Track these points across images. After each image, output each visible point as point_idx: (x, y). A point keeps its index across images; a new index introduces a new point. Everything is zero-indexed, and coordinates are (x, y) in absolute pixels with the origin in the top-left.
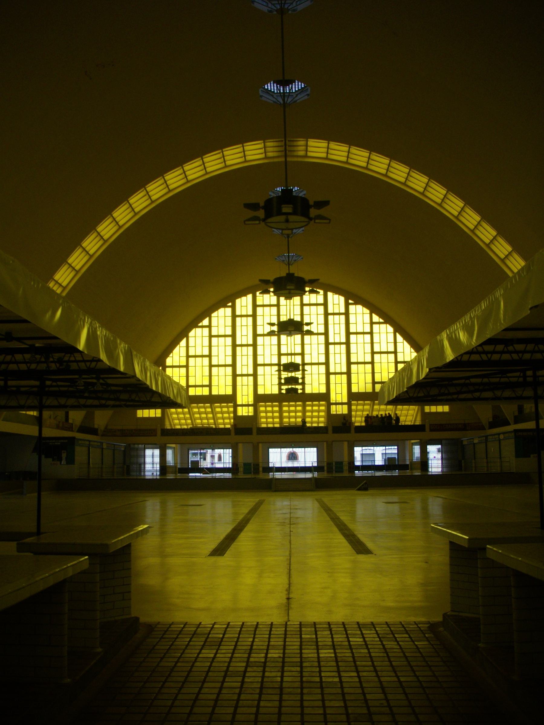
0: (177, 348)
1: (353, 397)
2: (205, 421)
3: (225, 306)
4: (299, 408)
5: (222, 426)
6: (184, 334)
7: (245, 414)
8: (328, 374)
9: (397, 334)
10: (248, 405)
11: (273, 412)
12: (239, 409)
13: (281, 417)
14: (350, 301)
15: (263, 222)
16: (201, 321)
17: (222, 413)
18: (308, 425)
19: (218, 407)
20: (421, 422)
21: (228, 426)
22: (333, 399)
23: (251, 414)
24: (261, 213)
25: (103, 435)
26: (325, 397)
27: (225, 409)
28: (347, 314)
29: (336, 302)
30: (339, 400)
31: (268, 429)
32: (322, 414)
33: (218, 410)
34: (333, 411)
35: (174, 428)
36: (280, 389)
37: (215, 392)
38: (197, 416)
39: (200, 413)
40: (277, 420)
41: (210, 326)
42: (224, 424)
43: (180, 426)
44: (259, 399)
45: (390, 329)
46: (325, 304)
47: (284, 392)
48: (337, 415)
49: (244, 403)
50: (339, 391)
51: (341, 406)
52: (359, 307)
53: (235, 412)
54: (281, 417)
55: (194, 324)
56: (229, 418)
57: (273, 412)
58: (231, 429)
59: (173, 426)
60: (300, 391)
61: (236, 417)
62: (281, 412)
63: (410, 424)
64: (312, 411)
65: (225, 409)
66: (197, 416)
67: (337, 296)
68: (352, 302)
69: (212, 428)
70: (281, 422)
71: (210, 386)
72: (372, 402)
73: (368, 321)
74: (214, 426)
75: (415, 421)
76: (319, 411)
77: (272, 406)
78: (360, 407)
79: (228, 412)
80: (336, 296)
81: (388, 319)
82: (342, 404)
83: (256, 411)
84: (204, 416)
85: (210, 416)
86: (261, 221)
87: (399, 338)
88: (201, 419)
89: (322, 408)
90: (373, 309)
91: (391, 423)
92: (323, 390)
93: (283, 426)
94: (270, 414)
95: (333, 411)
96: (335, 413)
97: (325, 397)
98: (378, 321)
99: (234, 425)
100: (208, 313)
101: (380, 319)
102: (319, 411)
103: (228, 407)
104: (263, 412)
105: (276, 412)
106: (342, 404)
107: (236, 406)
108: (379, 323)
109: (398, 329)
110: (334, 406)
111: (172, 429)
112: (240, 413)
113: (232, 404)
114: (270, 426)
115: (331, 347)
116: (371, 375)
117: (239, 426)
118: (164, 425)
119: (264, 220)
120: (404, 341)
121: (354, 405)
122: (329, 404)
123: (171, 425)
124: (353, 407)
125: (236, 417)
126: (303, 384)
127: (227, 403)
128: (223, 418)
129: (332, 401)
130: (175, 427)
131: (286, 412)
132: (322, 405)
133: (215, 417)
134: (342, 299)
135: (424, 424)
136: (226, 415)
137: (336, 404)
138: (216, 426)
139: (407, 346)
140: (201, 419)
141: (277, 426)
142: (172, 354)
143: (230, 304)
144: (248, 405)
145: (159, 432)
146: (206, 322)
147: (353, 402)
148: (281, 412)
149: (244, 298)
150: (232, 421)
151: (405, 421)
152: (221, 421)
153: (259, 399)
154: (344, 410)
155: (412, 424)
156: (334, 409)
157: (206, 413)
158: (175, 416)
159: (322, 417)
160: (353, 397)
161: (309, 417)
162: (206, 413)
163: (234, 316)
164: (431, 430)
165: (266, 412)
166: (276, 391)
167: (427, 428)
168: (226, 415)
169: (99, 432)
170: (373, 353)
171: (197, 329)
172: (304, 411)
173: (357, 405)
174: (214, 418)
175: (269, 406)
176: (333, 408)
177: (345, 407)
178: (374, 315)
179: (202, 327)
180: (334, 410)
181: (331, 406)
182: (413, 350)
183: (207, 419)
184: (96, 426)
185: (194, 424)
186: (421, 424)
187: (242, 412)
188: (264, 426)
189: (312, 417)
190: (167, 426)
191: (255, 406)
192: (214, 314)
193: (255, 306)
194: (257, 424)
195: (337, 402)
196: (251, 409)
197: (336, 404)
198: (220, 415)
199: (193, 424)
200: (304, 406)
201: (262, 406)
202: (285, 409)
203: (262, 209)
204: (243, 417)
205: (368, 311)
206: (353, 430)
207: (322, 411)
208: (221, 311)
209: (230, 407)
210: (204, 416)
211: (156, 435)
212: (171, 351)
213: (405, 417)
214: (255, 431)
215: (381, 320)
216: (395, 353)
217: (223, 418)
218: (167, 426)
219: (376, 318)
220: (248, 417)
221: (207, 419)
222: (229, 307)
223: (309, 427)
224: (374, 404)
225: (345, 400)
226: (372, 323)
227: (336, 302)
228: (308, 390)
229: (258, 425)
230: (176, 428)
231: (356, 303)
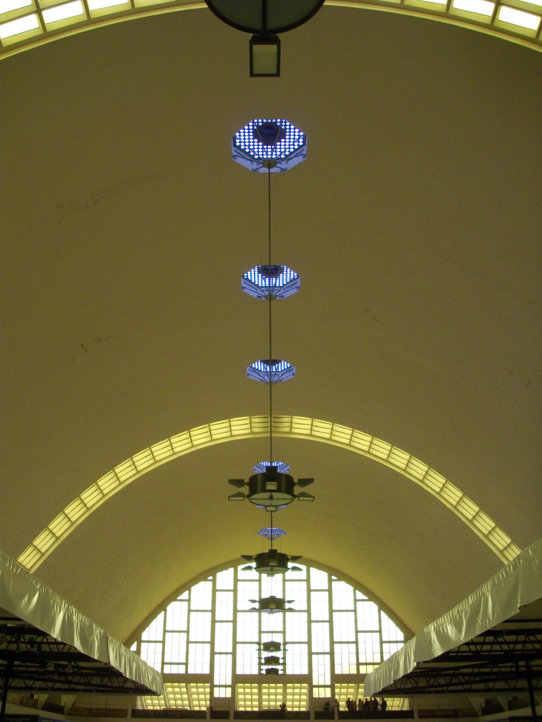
2: (179, 702)
3: (205, 579)
4: (280, 691)
5: (197, 709)
6: (162, 607)
7: (222, 695)
10: (226, 686)
11: (251, 694)
12: (216, 690)
13: (260, 700)
14: (334, 578)
15: (247, 498)
16: (180, 595)
17: (198, 693)
18: (289, 709)
19: (193, 687)
20: (408, 707)
21: (204, 709)
23: (229, 695)
24: (245, 490)
26: (307, 679)
27: (201, 690)
28: (330, 590)
31: (246, 713)
32: (304, 697)
33: (194, 690)
34: (315, 694)
35: (145, 709)
36: (260, 670)
37: (191, 671)
38: (171, 696)
39: (174, 693)
40: (256, 703)
41: (189, 601)
42: (200, 706)
43: (152, 707)
46: (308, 580)
47: (264, 672)
48: (319, 699)
49: (221, 684)
53: (212, 693)
54: (260, 700)
55: (173, 597)
56: (205, 700)
57: (251, 694)
58: (206, 712)
59: (145, 706)
60: (280, 672)
61: (212, 699)
62: (260, 694)
63: (397, 709)
64: (293, 694)
65: (201, 690)
66: (171, 696)
68: (336, 578)
69: (186, 711)
70: (260, 706)
71: (186, 664)
72: (356, 685)
74: (188, 708)
75: (402, 706)
76: (300, 694)
77: (251, 688)
78: (344, 690)
79: (205, 694)
81: (372, 596)
82: (325, 686)
83: (234, 692)
84: (178, 696)
85: (185, 696)
86: (245, 498)
88: (175, 700)
89: (304, 691)
90: (358, 585)
91: (377, 708)
92: (305, 672)
93: (262, 710)
94: (248, 697)
95: (315, 694)
96: (317, 696)
97: (307, 679)
98: (361, 598)
99: (211, 708)
100: (187, 586)
101: (364, 596)
102: (300, 694)
103: (204, 688)
104: (241, 694)
105: (255, 694)
106: (325, 686)
107: (212, 687)
108: (363, 600)
109: (383, 606)
111: (144, 710)
112: (216, 695)
113: (209, 684)
114: (249, 709)
117: (216, 709)
118: (136, 705)
119: (248, 497)
121: (338, 688)
122: (311, 687)
123: (143, 705)
124: (337, 690)
125: (212, 699)
126: (284, 664)
127: (204, 683)
128: (199, 700)
130: (147, 708)
131: (265, 694)
132: (304, 688)
133: (190, 697)
135: (412, 709)
136: (202, 696)
137: (319, 686)
138: (190, 708)
140: (175, 700)
141: (256, 709)
143: (211, 578)
144: (226, 686)
145: (129, 713)
146: (185, 595)
147: (336, 685)
148: (260, 694)
149: (225, 572)
150: (208, 703)
151: (392, 706)
152: (196, 703)
155: (399, 709)
157: (181, 693)
159: (303, 700)
161: (290, 700)
162: (181, 693)
163: (215, 590)
164: (420, 717)
165: (245, 694)
166: (255, 672)
167: (416, 714)
168: (202, 696)
169: (65, 710)
171: (175, 602)
172: (285, 694)
173: (341, 688)
174: (189, 699)
175: (248, 688)
176: (315, 690)
177: (328, 690)
178: (357, 591)
179: (181, 600)
180: (318, 693)
181: (314, 688)
183: (182, 699)
184: (62, 704)
185: (168, 705)
186: (409, 709)
187: (219, 693)
188: (242, 709)
189: (293, 701)
190: (138, 706)
191: (233, 687)
192: (194, 588)
193: (236, 580)
194: (234, 707)
196: (229, 690)
197: (319, 686)
198: (195, 696)
199: (166, 706)
200: (285, 689)
201: (241, 687)
202: (265, 691)
203: (247, 485)
204: (220, 699)
207: (304, 694)
208: (202, 584)
209: (207, 687)
210: (178, 696)
211: (126, 717)
213: (392, 702)
215: (366, 598)
217: (199, 700)
218: (138, 706)
219: (360, 595)
220: (225, 699)
221: (182, 699)
222: (210, 580)
223: (290, 712)
224: (358, 688)
225: (328, 682)
226: (356, 600)
228: (289, 672)
229: (235, 708)
230: (148, 709)
231: (339, 579)
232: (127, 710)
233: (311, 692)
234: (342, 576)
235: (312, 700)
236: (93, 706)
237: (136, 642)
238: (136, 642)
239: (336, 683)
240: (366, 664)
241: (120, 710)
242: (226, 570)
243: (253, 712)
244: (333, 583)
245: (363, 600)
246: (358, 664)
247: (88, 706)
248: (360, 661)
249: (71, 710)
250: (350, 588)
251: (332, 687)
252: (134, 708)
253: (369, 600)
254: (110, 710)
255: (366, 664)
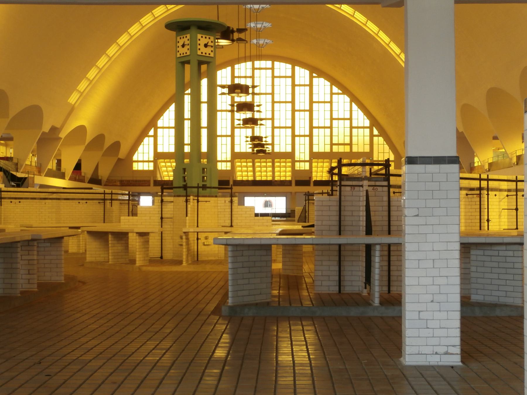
0: (167, 112)
1: (314, 156)
7: (224, 168)
8: (294, 136)
9: (353, 103)
10: (226, 161)
14: (314, 75)
22: (297, 158)
23: (229, 168)
25: (105, 185)
26: (290, 156)
28: (311, 85)
29: (302, 75)
30: (302, 159)
34: (297, 167)
43: (168, 178)
44: (236, 156)
45: (347, 99)
46: (293, 77)
47: (255, 151)
50: (302, 150)
51: (304, 163)
52: (322, 80)
67: (304, 69)
68: (316, 75)
73: (329, 91)
80: (302, 70)
81: (345, 91)
82: (305, 161)
83: (233, 166)
87: (355, 106)
90: (334, 82)
92: (289, 150)
96: (298, 169)
97: (290, 156)
98: (337, 92)
101: (339, 90)
106: (305, 161)
108: (338, 94)
109: (354, 99)
110: (298, 163)
115: (297, 113)
116: (329, 138)
118: (156, 177)
120: (359, 109)
122: (294, 162)
123: (161, 177)
126: (273, 144)
129: (297, 158)
134: (307, 72)
137: (300, 161)
139: (361, 114)
142: (162, 117)
144: (226, 161)
149: (224, 70)
153: (236, 156)
154: (307, 166)
156: (298, 166)
158: (165, 169)
160: (314, 156)
166: (250, 150)
170: (332, 119)
176: (297, 165)
177: (307, 164)
178: (334, 87)
180: (298, 166)
182: (365, 117)
188: (239, 178)
191: (232, 162)
194: (233, 177)
195: (301, 160)
196: (229, 164)
197: (300, 161)
202: (257, 164)
205: (329, 84)
206: (312, 184)
211: (149, 186)
212: (162, 115)
214: (231, 183)
215: (340, 92)
216: (351, 119)
219: (335, 89)
225: (307, 158)
226: (332, 94)
227: (302, 75)
228: (277, 150)
231: (319, 76)
232: (150, 180)
233: (293, 166)
234: (321, 74)
235: (294, 171)
236: (124, 179)
237: (153, 129)
238: (153, 129)
239: (313, 159)
240: (338, 144)
241: (144, 181)
242: (225, 68)
243: (248, 181)
244: (314, 79)
245: (338, 94)
246: (332, 144)
247: (120, 179)
248: (334, 142)
249: (106, 182)
250: (328, 83)
251: (310, 162)
252: (155, 179)
253: (343, 93)
254: (136, 181)
255: (338, 144)
